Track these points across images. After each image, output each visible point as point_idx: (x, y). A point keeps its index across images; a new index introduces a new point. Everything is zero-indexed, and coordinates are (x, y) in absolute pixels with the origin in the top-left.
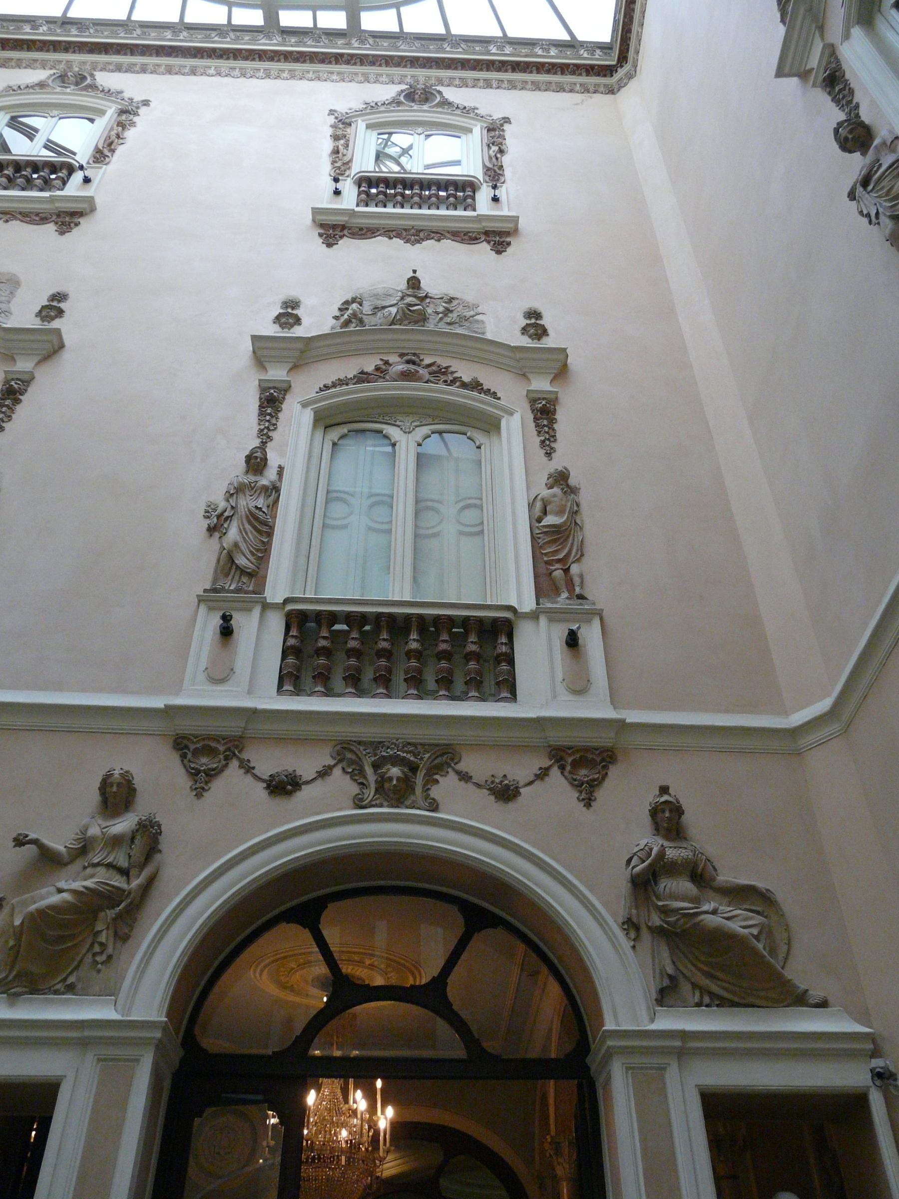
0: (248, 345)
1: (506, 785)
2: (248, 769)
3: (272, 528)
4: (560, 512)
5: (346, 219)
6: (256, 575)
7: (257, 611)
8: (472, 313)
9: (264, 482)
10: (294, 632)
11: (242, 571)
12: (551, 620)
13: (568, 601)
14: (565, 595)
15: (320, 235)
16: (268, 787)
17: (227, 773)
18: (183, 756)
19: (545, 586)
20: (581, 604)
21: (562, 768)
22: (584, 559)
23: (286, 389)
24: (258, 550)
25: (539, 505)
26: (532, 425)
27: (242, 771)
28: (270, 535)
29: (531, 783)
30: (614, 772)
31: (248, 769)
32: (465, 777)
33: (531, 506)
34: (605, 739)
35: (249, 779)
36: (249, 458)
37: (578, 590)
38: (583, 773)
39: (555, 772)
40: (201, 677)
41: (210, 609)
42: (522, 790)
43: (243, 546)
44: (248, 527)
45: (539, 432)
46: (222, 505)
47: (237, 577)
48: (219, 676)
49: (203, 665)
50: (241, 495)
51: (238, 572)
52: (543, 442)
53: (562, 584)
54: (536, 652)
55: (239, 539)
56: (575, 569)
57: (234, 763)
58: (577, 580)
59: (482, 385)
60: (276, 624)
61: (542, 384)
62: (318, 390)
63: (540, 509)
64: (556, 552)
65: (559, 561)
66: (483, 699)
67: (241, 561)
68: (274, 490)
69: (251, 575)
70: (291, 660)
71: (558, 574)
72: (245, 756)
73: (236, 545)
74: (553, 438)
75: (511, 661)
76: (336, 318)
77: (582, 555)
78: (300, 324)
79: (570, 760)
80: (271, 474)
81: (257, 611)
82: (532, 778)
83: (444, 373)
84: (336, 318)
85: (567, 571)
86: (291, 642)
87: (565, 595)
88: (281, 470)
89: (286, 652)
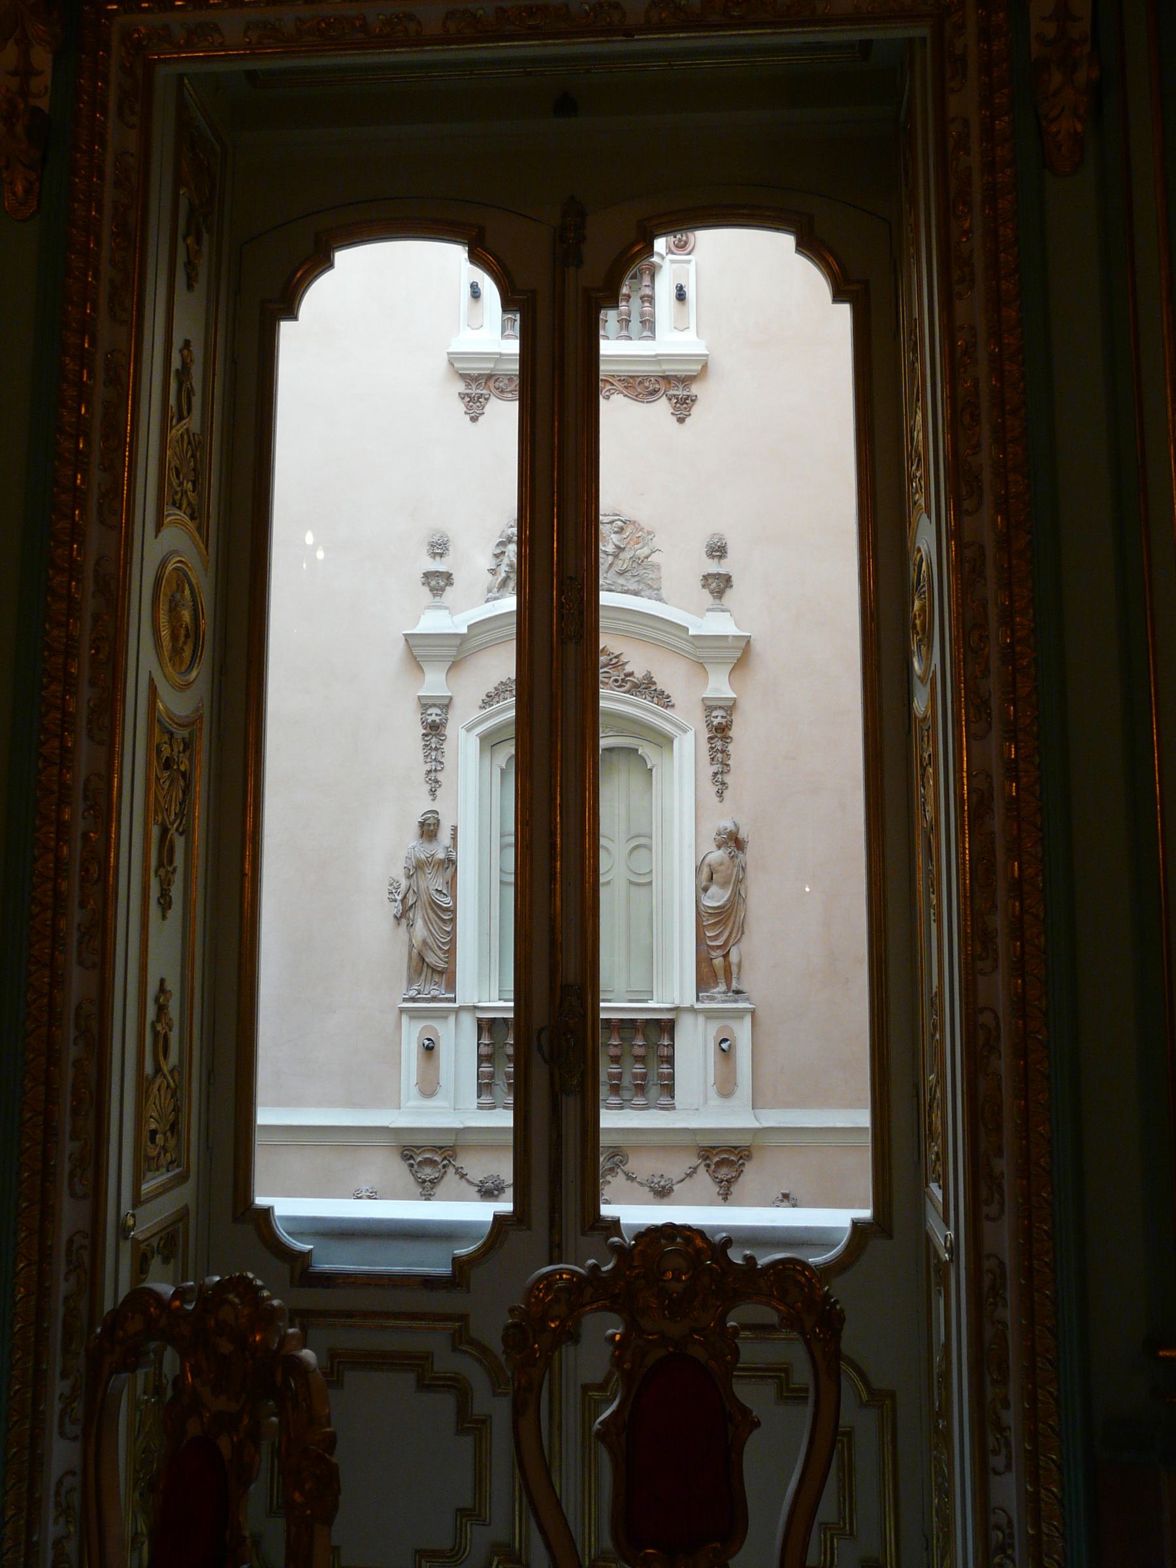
0: (402, 642)
1: (663, 1187)
2: (463, 1176)
3: (453, 911)
4: (724, 885)
5: (491, 365)
6: (447, 975)
7: (452, 1019)
8: (646, 551)
9: (441, 855)
10: (485, 1035)
11: (434, 970)
12: (707, 1018)
13: (723, 997)
14: (722, 987)
15: (462, 396)
16: (479, 1191)
17: (446, 1179)
18: (412, 1165)
19: (706, 977)
20: (736, 1001)
21: (708, 1166)
22: (744, 937)
23: (446, 705)
24: (443, 944)
25: (705, 872)
26: (705, 746)
27: (458, 1176)
28: (453, 920)
29: (682, 1180)
30: (749, 1168)
31: (463, 1176)
32: (630, 1178)
33: (698, 870)
34: (743, 1141)
35: (464, 1183)
36: (422, 824)
37: (734, 985)
38: (724, 1173)
39: (702, 1169)
40: (414, 1091)
41: (411, 1018)
42: (675, 1187)
43: (430, 941)
44: (432, 915)
45: (712, 759)
46: (404, 883)
47: (429, 975)
48: (428, 1088)
49: (414, 1080)
50: (420, 873)
51: (430, 971)
52: (716, 774)
53: (721, 973)
54: (692, 1049)
55: (426, 933)
56: (734, 957)
57: (451, 1170)
58: (734, 969)
59: (654, 683)
60: (469, 1025)
61: (719, 686)
62: (480, 703)
63: (707, 877)
64: (716, 938)
65: (719, 947)
66: (645, 1107)
67: (431, 958)
68: (450, 863)
69: (441, 973)
70: (486, 1068)
71: (718, 962)
72: (458, 1165)
73: (425, 943)
74: (725, 768)
75: (670, 1060)
76: (493, 572)
77: (743, 933)
78: (452, 584)
79: (716, 1159)
80: (444, 836)
81: (452, 1019)
82: (683, 1176)
83: (615, 666)
84: (493, 572)
85: (726, 956)
86: (485, 1051)
87: (722, 987)
88: (455, 829)
89: (481, 1059)
